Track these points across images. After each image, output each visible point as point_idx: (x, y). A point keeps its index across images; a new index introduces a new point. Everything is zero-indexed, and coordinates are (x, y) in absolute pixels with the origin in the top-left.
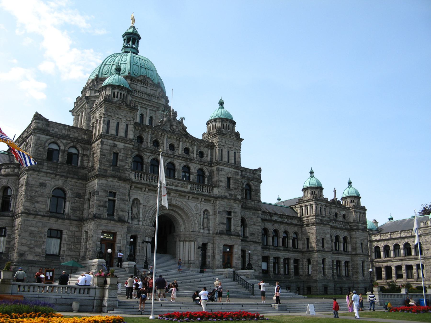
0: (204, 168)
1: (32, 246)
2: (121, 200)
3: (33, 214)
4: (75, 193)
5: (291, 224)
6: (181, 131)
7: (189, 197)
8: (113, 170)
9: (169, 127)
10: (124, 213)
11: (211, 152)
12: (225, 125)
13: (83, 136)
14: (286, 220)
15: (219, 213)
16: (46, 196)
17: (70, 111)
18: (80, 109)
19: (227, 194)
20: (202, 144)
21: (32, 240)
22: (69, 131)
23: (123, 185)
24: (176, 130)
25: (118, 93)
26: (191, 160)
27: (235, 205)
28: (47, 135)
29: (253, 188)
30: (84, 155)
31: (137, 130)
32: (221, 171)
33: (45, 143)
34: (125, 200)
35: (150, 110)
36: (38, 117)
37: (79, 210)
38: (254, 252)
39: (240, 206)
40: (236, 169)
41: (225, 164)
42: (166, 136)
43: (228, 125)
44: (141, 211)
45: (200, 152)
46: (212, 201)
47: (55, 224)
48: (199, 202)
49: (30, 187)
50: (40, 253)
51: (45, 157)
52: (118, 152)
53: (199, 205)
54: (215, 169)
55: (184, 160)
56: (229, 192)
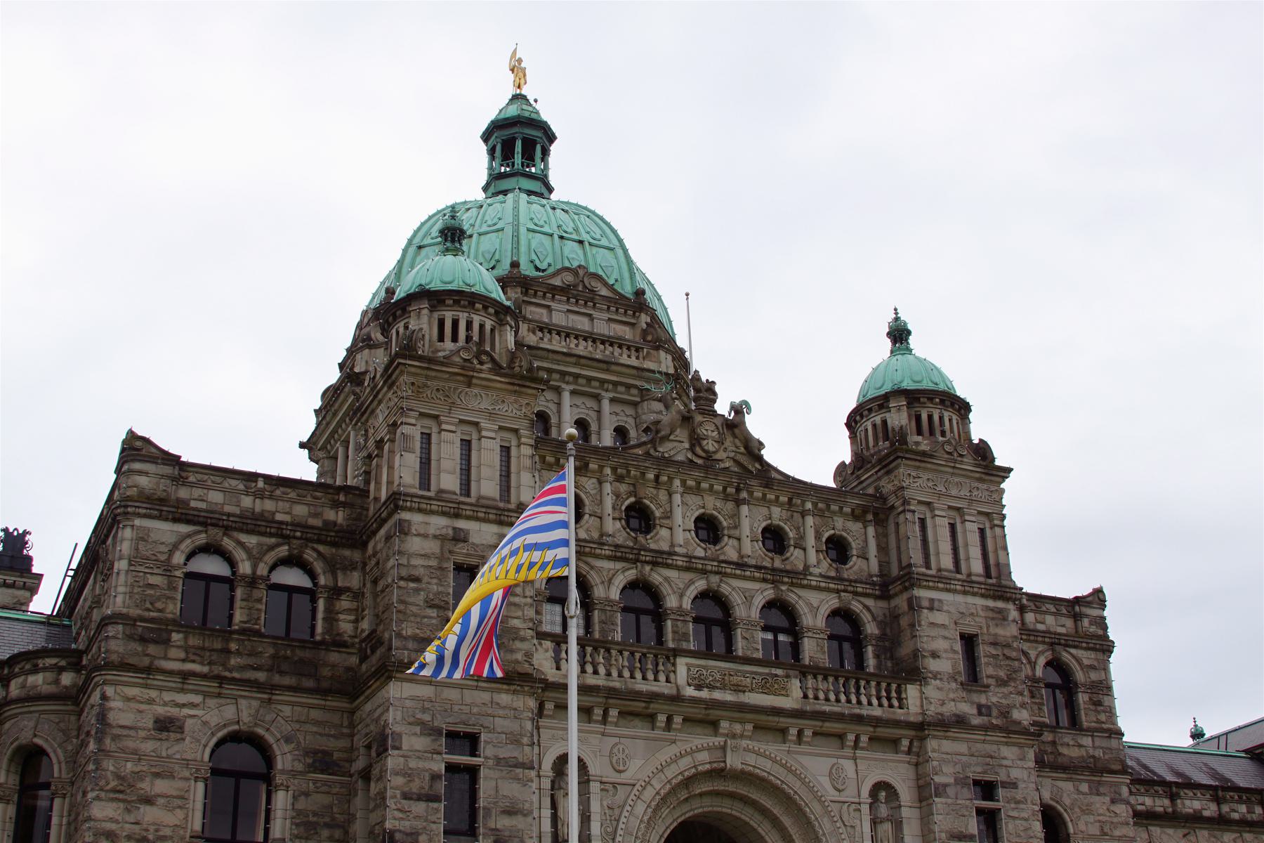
0: (856, 606)
2: (499, 761)
4: (307, 753)
6: (739, 457)
7: (800, 733)
9: (687, 445)
10: (520, 818)
11: (877, 536)
13: (330, 515)
15: (941, 790)
16: (186, 774)
17: (302, 445)
18: (334, 431)
19: (967, 709)
20: (834, 507)
22: (271, 497)
24: (717, 456)
25: (455, 323)
26: (798, 577)
27: (1009, 752)
28: (176, 520)
29: (1080, 676)
30: (336, 592)
32: (931, 609)
33: (171, 553)
35: (612, 400)
36: (136, 450)
37: (327, 825)
39: (1031, 754)
40: (995, 598)
42: (677, 482)
43: (936, 418)
44: (595, 807)
45: (829, 540)
46: (905, 742)
48: (848, 752)
49: (116, 738)
51: (173, 609)
52: (473, 561)
53: (848, 765)
54: (905, 606)
55: (764, 580)
56: (976, 697)
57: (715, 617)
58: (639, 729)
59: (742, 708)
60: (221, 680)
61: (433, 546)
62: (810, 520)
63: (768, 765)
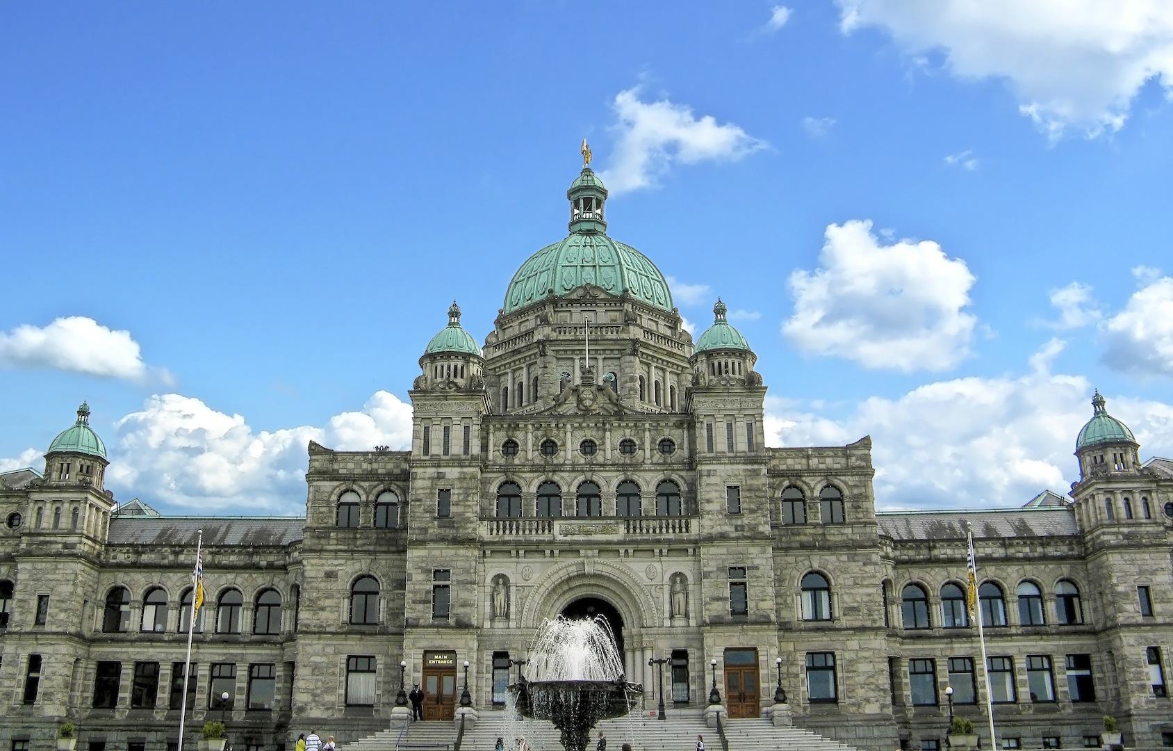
0: (675, 477)
1: (319, 691)
2: (458, 582)
3: (315, 633)
4: (393, 581)
5: (1044, 558)
8: (440, 527)
12: (716, 364)
14: (1027, 550)
15: (707, 575)
19: (728, 529)
20: (663, 424)
21: (317, 681)
23: (462, 552)
29: (846, 492)
31: (499, 429)
32: (709, 476)
34: (471, 583)
38: (861, 654)
40: (752, 463)
41: (718, 459)
42: (569, 426)
44: (513, 598)
46: (691, 551)
47: (356, 646)
50: (333, 704)
51: (332, 521)
53: (657, 565)
56: (734, 522)
57: (589, 494)
58: (538, 559)
59: (589, 543)
60: (352, 552)
61: (428, 483)
62: (647, 434)
63: (609, 569)
